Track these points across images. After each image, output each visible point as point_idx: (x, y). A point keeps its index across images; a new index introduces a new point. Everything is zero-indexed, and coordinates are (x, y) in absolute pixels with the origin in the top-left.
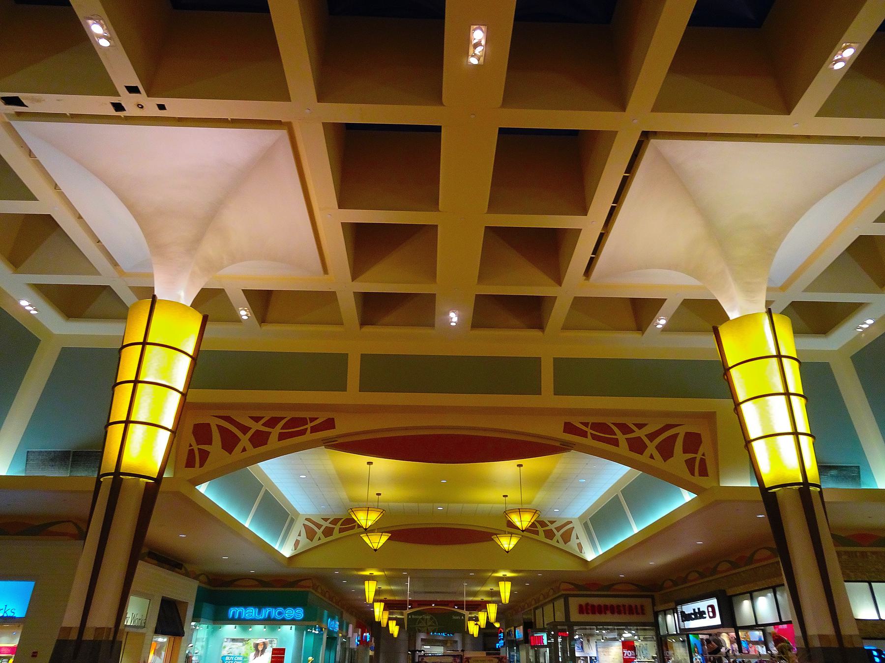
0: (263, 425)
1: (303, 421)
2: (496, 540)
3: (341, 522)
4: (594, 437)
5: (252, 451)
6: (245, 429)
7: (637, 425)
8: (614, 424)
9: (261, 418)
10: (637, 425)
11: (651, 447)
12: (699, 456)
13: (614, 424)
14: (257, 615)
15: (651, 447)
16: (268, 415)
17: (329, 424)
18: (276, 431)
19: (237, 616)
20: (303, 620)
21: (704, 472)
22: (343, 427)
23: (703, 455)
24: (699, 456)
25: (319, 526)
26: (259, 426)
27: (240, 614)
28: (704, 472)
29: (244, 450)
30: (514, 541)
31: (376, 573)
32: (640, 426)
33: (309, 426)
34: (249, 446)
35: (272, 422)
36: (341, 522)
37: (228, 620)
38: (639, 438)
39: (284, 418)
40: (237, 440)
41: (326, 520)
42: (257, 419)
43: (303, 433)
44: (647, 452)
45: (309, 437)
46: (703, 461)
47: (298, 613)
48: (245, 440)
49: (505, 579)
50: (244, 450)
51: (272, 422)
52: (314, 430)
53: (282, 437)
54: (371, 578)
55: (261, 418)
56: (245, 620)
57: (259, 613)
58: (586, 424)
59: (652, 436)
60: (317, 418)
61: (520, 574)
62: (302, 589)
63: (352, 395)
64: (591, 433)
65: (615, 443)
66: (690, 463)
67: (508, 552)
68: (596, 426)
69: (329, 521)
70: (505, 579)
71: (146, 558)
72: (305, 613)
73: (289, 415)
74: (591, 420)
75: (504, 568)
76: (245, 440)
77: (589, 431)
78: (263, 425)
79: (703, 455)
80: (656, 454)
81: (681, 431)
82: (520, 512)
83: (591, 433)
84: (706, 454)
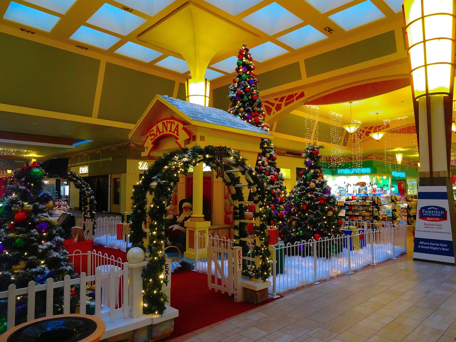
0: (279, 101)
1: (292, 96)
3: (373, 128)
5: (277, 113)
6: (273, 105)
9: (278, 98)
14: (349, 172)
16: (280, 97)
17: (302, 95)
18: (283, 103)
19: (341, 173)
20: (370, 173)
22: (308, 94)
25: (363, 132)
26: (277, 103)
27: (343, 172)
29: (274, 113)
31: (402, 150)
33: (295, 97)
34: (275, 111)
35: (281, 100)
36: (373, 128)
37: (338, 174)
39: (285, 96)
40: (271, 110)
41: (366, 128)
42: (276, 99)
43: (293, 101)
45: (295, 102)
47: (368, 170)
48: (274, 109)
50: (274, 113)
51: (281, 100)
52: (297, 99)
53: (286, 104)
54: (398, 152)
55: (278, 98)
56: (345, 174)
57: (351, 171)
60: (297, 93)
62: (368, 160)
63: (305, 80)
69: (368, 129)
71: (286, 154)
72: (371, 170)
73: (287, 94)
76: (274, 109)
78: (279, 101)
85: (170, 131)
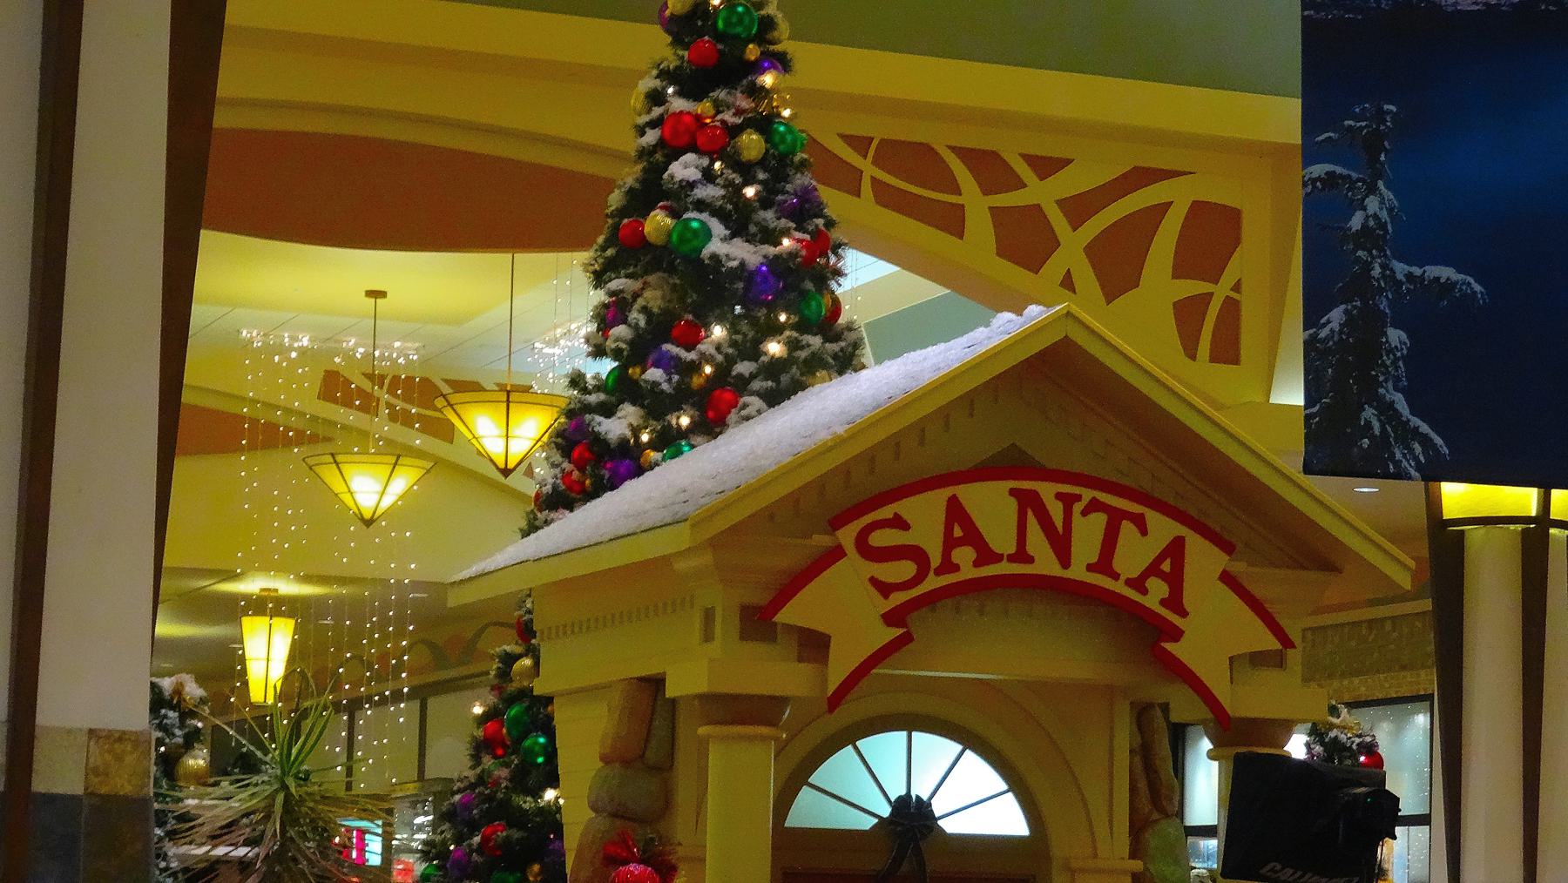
2: (330, 475)
4: (887, 197)
7: (1032, 161)
8: (961, 152)
10: (1032, 161)
11: (1072, 246)
12: (1221, 291)
13: (961, 152)
15: (1072, 246)
21: (1227, 351)
23: (1237, 287)
24: (1221, 291)
28: (1227, 351)
30: (402, 482)
32: (1046, 166)
38: (1037, 208)
44: (1055, 266)
46: (1231, 308)
49: (263, 605)
58: (860, 144)
59: (1079, 209)
61: (335, 590)
64: (874, 179)
65: (952, 221)
66: (1188, 314)
67: (368, 523)
68: (893, 154)
70: (263, 605)
74: (878, 129)
75: (267, 567)
77: (868, 169)
79: (1237, 287)
80: (1086, 277)
81: (1179, 196)
82: (508, 401)
83: (874, 179)
84: (1244, 287)
85: (1104, 564)
